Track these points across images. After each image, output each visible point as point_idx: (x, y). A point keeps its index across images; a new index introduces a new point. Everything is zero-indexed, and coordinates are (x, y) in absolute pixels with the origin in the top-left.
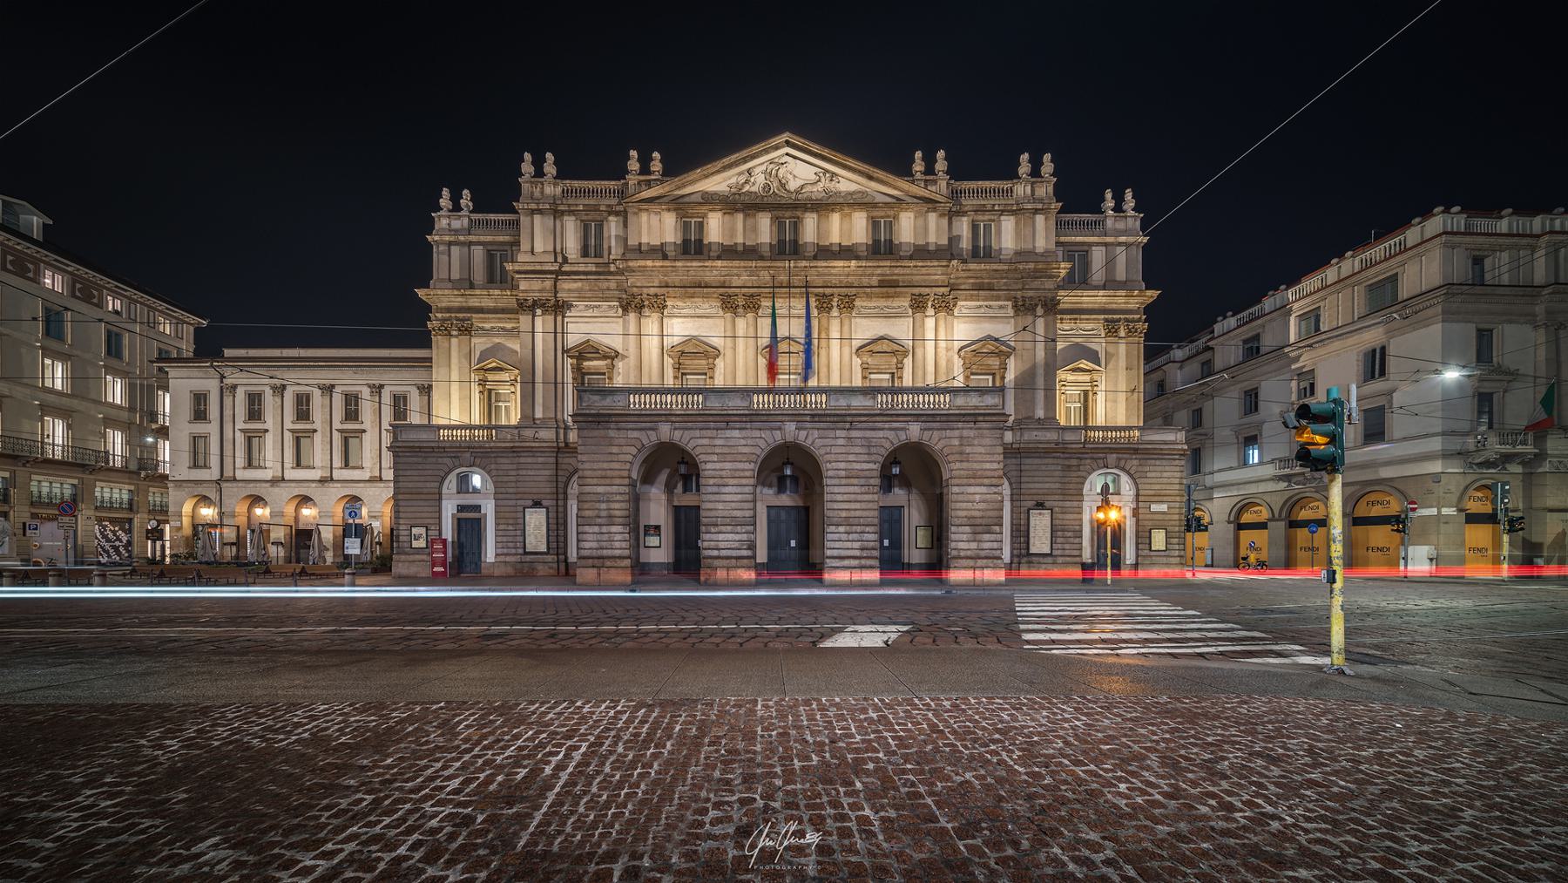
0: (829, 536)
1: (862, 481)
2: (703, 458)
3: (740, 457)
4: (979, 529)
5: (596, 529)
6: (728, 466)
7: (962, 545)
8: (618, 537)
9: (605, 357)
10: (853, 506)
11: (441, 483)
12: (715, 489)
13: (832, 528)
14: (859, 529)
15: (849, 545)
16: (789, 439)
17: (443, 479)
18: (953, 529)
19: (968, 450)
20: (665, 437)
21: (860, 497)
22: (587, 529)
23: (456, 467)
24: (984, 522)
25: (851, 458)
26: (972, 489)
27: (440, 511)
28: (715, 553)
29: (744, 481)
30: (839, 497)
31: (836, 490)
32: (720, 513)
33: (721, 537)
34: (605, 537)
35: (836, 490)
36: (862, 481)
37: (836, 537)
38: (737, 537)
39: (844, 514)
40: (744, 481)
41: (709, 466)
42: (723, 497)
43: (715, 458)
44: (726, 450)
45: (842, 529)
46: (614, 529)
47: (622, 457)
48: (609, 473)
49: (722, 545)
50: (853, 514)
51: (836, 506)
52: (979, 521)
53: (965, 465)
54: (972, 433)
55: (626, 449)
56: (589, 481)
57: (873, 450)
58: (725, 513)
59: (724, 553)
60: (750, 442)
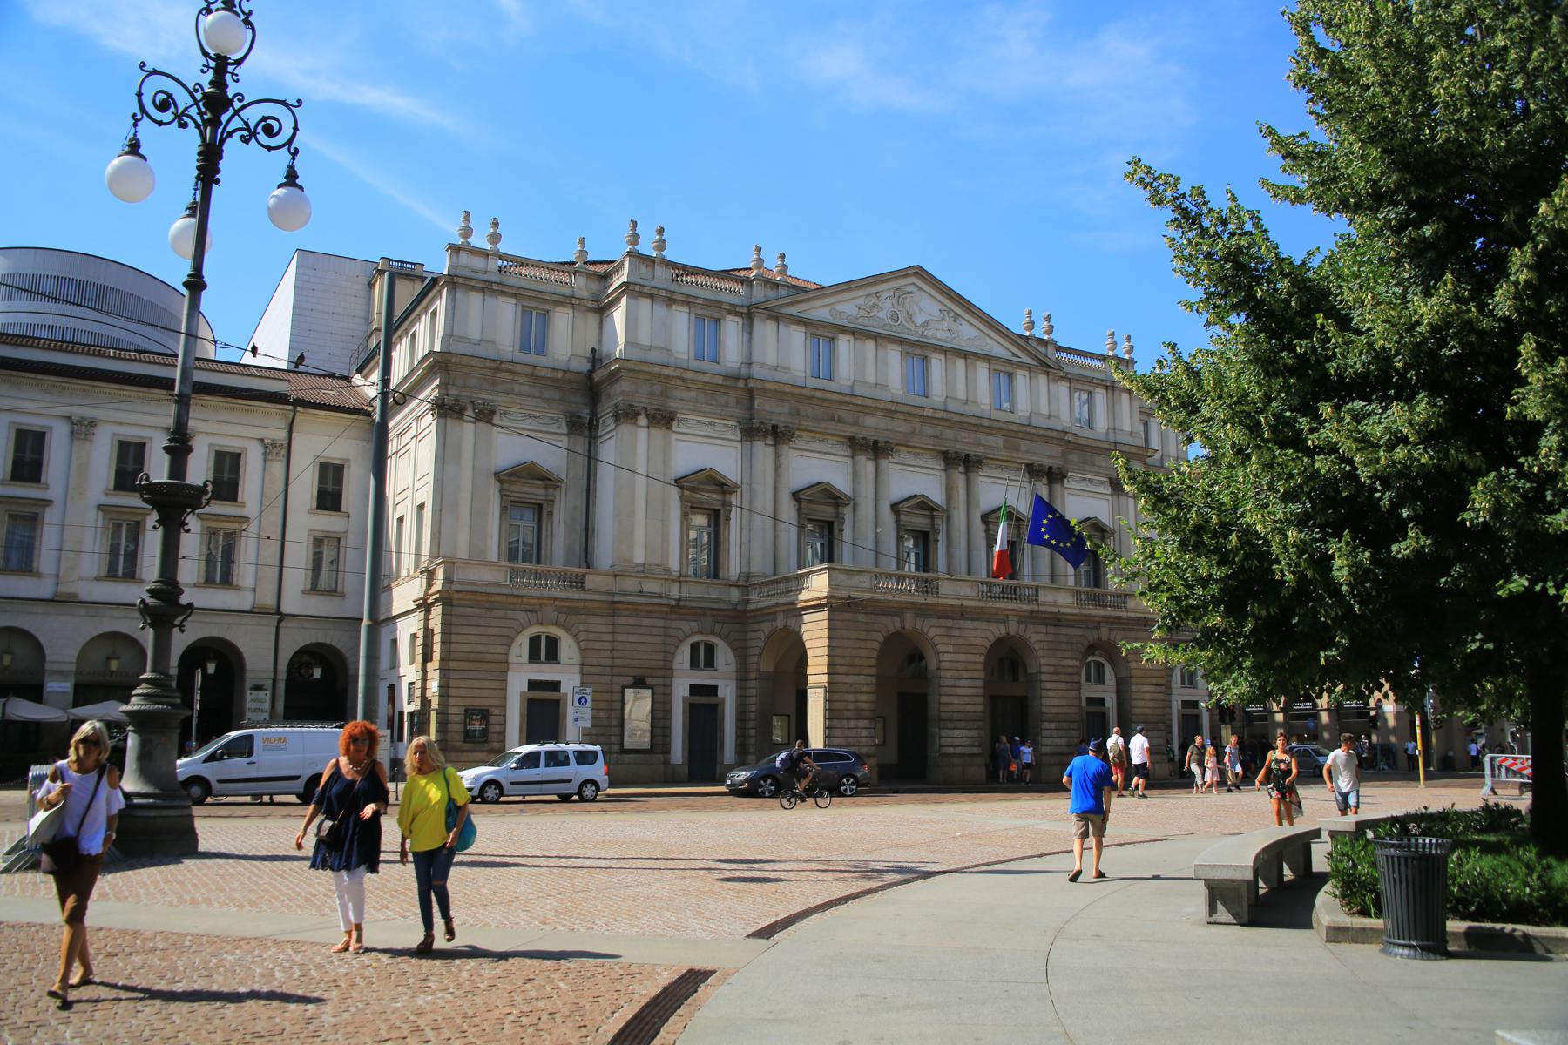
0: (1045, 733)
1: (1067, 678)
2: (941, 648)
6: (962, 657)
8: (865, 733)
11: (509, 646)
13: (1046, 725)
15: (1058, 741)
16: (1012, 632)
17: (513, 639)
23: (530, 624)
25: (1059, 654)
27: (505, 689)
28: (951, 750)
29: (976, 675)
30: (1051, 694)
31: (1048, 685)
32: (955, 708)
33: (956, 733)
35: (1048, 685)
36: (1067, 678)
38: (970, 733)
39: (1054, 710)
40: (976, 675)
43: (951, 649)
44: (960, 641)
45: (1053, 725)
46: (862, 723)
48: (857, 661)
49: (957, 742)
58: (961, 708)
59: (959, 750)
60: (980, 634)
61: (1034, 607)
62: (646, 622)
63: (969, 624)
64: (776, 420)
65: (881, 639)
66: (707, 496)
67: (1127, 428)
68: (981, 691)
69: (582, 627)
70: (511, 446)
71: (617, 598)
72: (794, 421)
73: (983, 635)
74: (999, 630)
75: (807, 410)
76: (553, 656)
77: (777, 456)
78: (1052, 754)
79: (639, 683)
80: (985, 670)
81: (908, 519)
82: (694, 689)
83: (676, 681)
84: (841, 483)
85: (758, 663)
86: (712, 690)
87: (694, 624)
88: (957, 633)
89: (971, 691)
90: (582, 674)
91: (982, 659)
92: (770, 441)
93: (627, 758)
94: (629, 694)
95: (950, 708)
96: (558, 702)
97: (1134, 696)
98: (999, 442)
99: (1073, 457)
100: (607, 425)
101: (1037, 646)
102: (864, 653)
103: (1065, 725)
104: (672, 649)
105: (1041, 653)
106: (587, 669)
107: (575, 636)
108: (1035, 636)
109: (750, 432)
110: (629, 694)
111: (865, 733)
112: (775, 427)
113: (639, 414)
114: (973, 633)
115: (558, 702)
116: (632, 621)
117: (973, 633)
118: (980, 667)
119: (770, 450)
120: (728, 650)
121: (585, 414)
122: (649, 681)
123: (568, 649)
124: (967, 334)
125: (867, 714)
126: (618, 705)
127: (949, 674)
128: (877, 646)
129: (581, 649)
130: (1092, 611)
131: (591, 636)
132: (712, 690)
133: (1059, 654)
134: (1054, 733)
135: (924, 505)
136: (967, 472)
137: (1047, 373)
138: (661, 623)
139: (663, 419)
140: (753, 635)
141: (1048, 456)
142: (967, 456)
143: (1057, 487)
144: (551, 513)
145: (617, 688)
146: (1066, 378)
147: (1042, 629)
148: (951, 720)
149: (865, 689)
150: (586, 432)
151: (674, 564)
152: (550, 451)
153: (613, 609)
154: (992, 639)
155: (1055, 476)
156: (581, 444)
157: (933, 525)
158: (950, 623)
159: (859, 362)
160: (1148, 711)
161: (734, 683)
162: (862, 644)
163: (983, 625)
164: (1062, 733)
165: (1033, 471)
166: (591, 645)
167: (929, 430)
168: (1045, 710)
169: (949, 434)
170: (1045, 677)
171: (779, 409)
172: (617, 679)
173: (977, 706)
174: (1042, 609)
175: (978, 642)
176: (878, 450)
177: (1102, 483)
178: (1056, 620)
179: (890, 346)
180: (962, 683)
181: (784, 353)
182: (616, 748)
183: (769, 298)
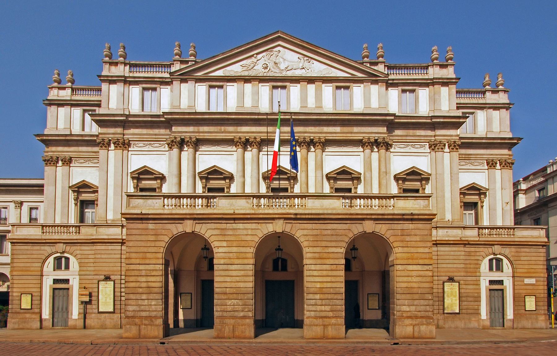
10: (325, 279)
12: (225, 267)
13: (311, 296)
14: (330, 296)
15: (323, 308)
21: (330, 273)
30: (315, 273)
31: (313, 267)
32: (228, 285)
33: (229, 302)
35: (313, 267)
37: (313, 302)
39: (318, 285)
42: (231, 273)
45: (318, 296)
50: (325, 285)
51: (312, 279)
58: (233, 285)
75: (206, 129)
78: (316, 317)
89: (242, 273)
113: (109, 145)
118: (250, 255)
127: (222, 261)
134: (319, 302)
139: (124, 145)
148: (225, 293)
164: (327, 302)
180: (233, 267)
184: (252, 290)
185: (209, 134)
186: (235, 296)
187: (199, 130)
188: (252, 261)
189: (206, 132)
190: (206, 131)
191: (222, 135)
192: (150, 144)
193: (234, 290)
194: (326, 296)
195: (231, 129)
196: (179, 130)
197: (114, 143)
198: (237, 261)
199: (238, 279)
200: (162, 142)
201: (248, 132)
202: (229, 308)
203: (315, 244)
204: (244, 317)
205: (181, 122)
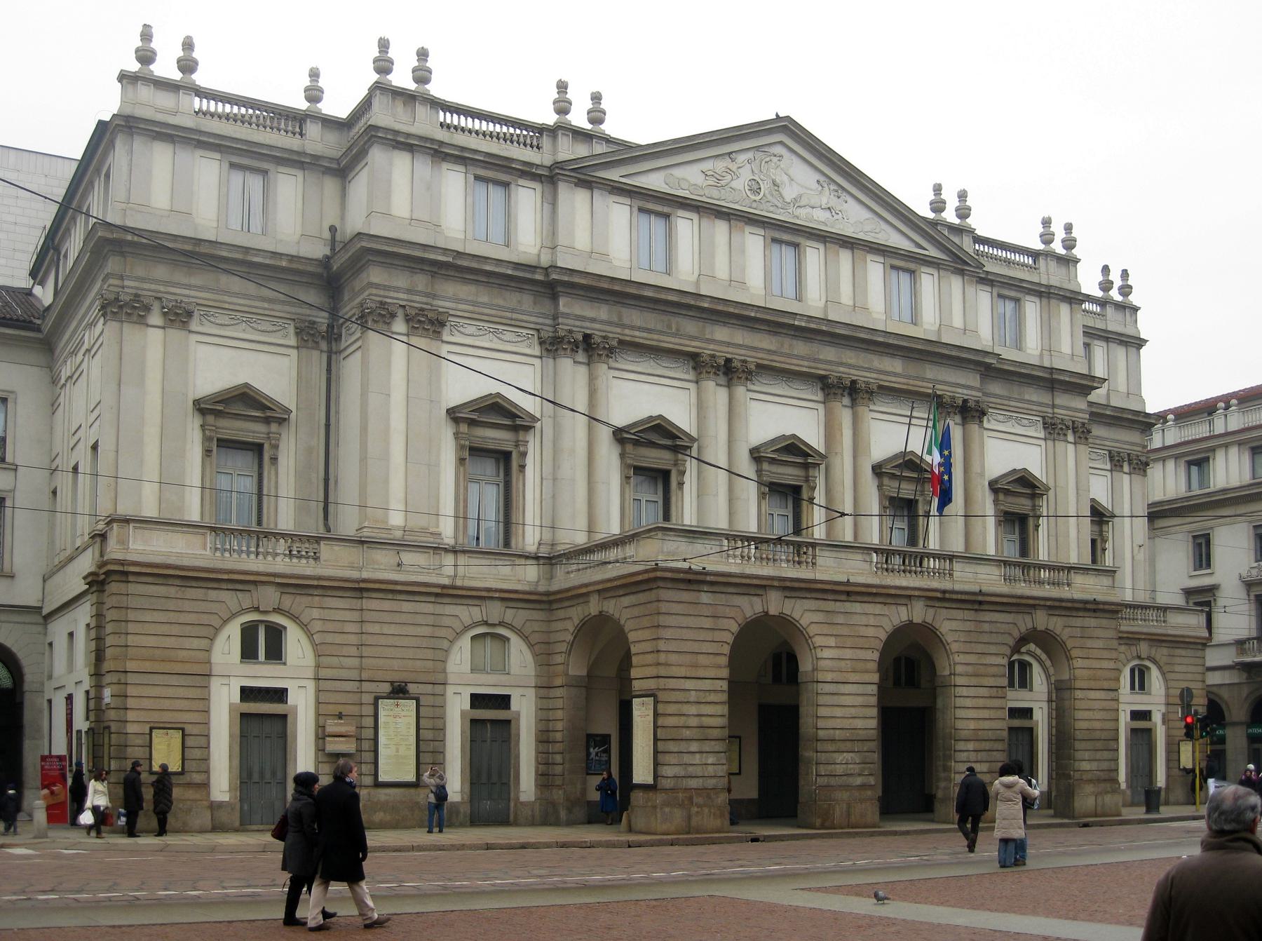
3: (861, 642)
4: (1099, 745)
5: (683, 746)
6: (848, 654)
7: (1085, 766)
8: (711, 759)
9: (516, 429)
13: (961, 746)
16: (917, 619)
18: (1078, 745)
19: (1089, 643)
20: (773, 611)
22: (672, 746)
24: (1104, 735)
25: (980, 648)
26: (1093, 694)
30: (968, 702)
31: (964, 691)
33: (840, 758)
34: (697, 759)
39: (972, 725)
41: (826, 653)
43: (832, 642)
44: (845, 631)
45: (971, 746)
46: (707, 746)
47: (719, 636)
52: (1097, 735)
53: (1086, 663)
54: (1092, 622)
55: (724, 623)
56: (675, 671)
57: (1000, 639)
58: (846, 724)
60: (872, 621)
61: (946, 585)
62: (406, 606)
63: (857, 607)
64: (590, 328)
65: (735, 628)
66: (492, 437)
67: (1066, 348)
68: (874, 700)
69: (316, 613)
70: (226, 359)
71: (365, 575)
72: (615, 333)
73: (879, 623)
74: (900, 615)
75: (634, 317)
76: (275, 653)
77: (592, 379)
79: (399, 691)
80: (879, 670)
81: (774, 468)
82: (478, 700)
83: (450, 690)
84: (680, 414)
85: (566, 664)
86: (503, 701)
87: (476, 613)
88: (840, 619)
89: (860, 700)
90: (317, 679)
91: (876, 656)
92: (581, 356)
93: (383, 794)
94: (385, 707)
95: (830, 723)
96: (285, 717)
97: (1078, 704)
98: (895, 365)
99: (996, 388)
100: (352, 334)
101: (949, 638)
102: (707, 647)
103: (987, 745)
104: (445, 644)
105: (955, 647)
106: (323, 673)
107: (304, 626)
108: (950, 625)
109: (553, 345)
110: (385, 707)
111: (710, 761)
112: (587, 337)
114: (864, 620)
115: (285, 717)
116: (387, 605)
117: (864, 620)
118: (874, 666)
119: (582, 371)
120: (524, 647)
121: (322, 319)
122: (412, 688)
123: (296, 644)
124: (854, 218)
125: (716, 733)
126: (369, 722)
127: (829, 677)
128: (730, 638)
129: (315, 645)
130: (1022, 589)
131: (330, 627)
132: (503, 701)
133: (980, 648)
135: (793, 449)
136: (853, 405)
137: (961, 272)
138: (429, 608)
139: (429, 324)
140: (560, 625)
141: (962, 384)
142: (854, 382)
143: (974, 427)
144: (274, 460)
145: (368, 699)
146: (987, 280)
147: (959, 614)
149: (712, 698)
150: (324, 345)
151: (447, 530)
152: (273, 371)
153: (360, 589)
154: (889, 628)
155: (971, 413)
156: (317, 360)
157: (807, 480)
158: (831, 606)
159: (704, 251)
160: (1097, 725)
161: (531, 693)
162: (709, 636)
163: (878, 609)
165: (941, 405)
166: (329, 638)
167: (801, 347)
168: (959, 724)
169: (829, 353)
170: (959, 680)
171: (589, 313)
172: (366, 686)
173: (869, 722)
174: (957, 587)
175: (871, 632)
176: (730, 372)
177: (1032, 424)
178: (976, 602)
179: (748, 229)
181: (604, 237)
182: (368, 780)
183: (577, 159)
184: (874, 734)
185: (645, 335)
186: (849, 744)
187: (620, 318)
188: (875, 678)
189: (639, 329)
190: (638, 322)
191: (673, 340)
192: (496, 332)
193: (847, 734)
194: (987, 745)
195: (690, 327)
196: (579, 314)
197: (408, 319)
198: (853, 677)
199: (853, 711)
200: (525, 331)
201: (729, 344)
202: (839, 769)
203: (968, 648)
204: (863, 787)
205: (581, 293)
